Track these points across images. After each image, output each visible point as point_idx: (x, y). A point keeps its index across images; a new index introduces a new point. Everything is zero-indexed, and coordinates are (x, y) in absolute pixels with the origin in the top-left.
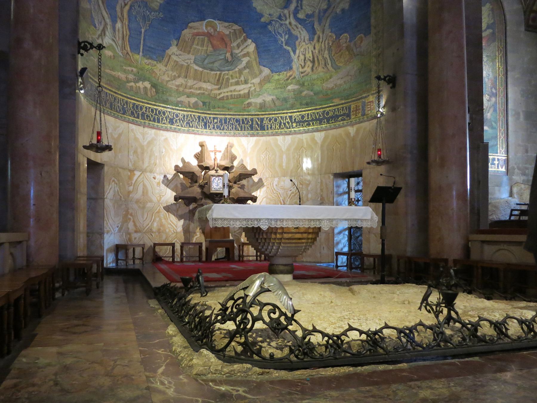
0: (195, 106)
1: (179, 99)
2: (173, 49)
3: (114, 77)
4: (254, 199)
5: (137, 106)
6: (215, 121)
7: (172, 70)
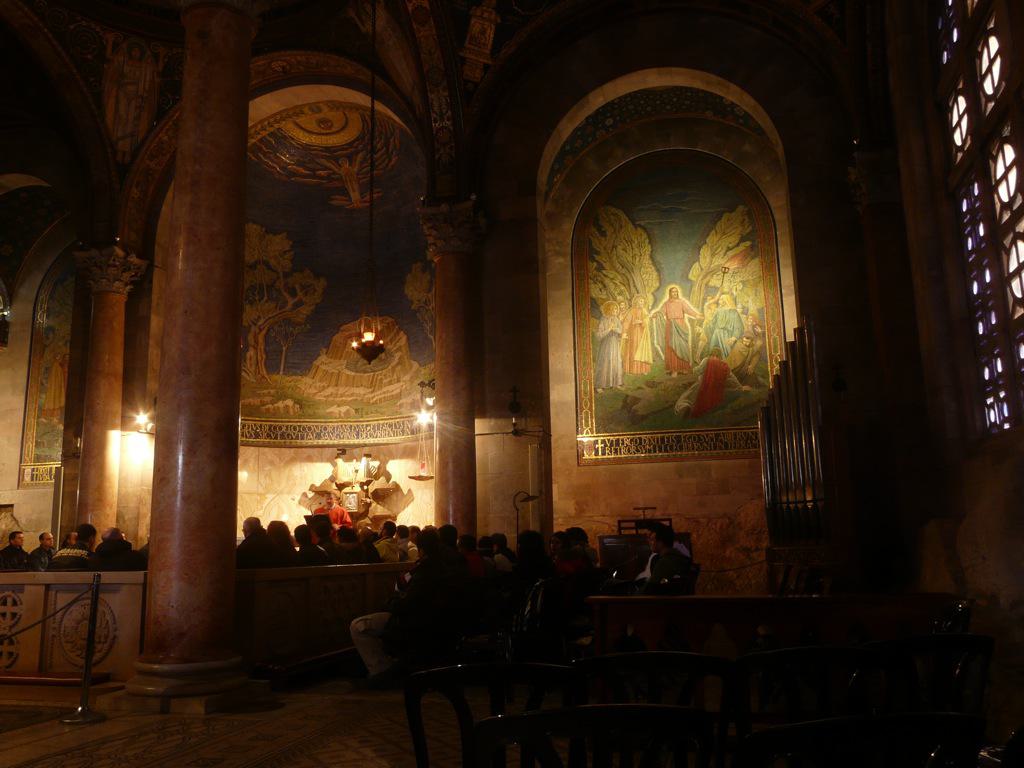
0: (347, 413)
1: (328, 411)
2: (323, 358)
5: (275, 428)
6: (368, 428)
7: (320, 381)
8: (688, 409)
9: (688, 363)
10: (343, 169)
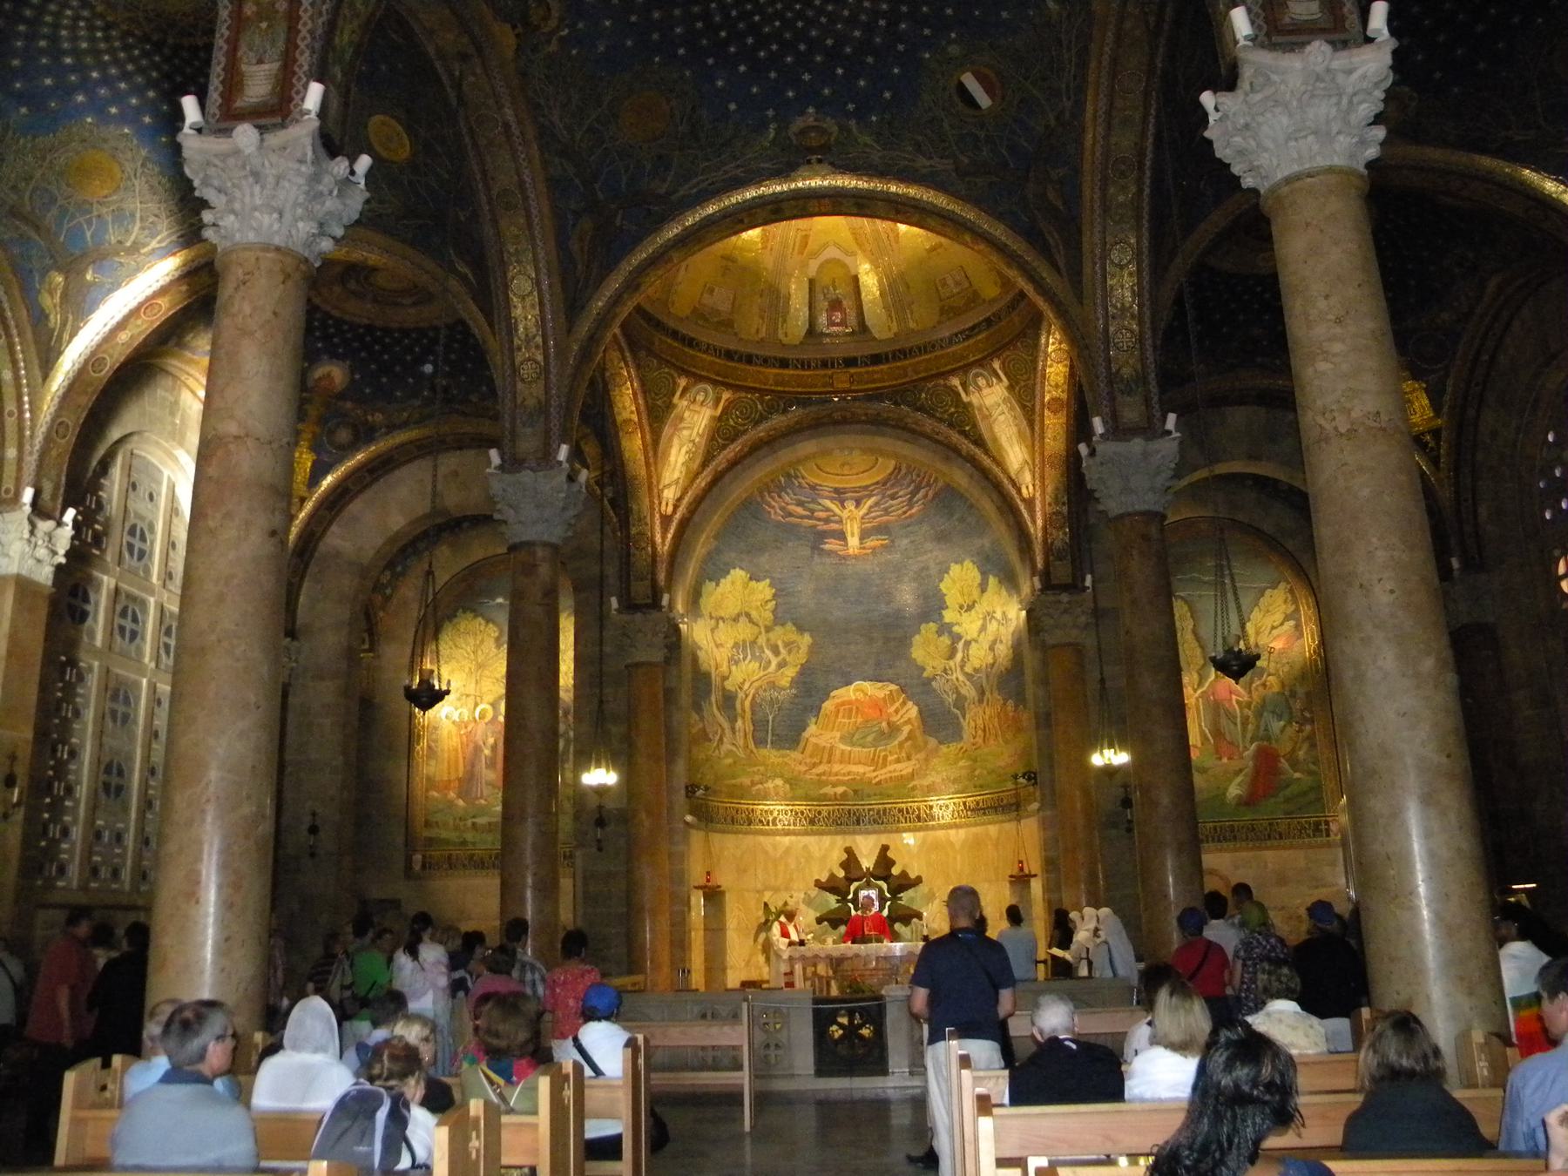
0: (844, 795)
2: (812, 729)
3: (734, 785)
4: (919, 916)
7: (811, 756)
8: (1240, 797)
9: (1238, 747)
10: (846, 511)
